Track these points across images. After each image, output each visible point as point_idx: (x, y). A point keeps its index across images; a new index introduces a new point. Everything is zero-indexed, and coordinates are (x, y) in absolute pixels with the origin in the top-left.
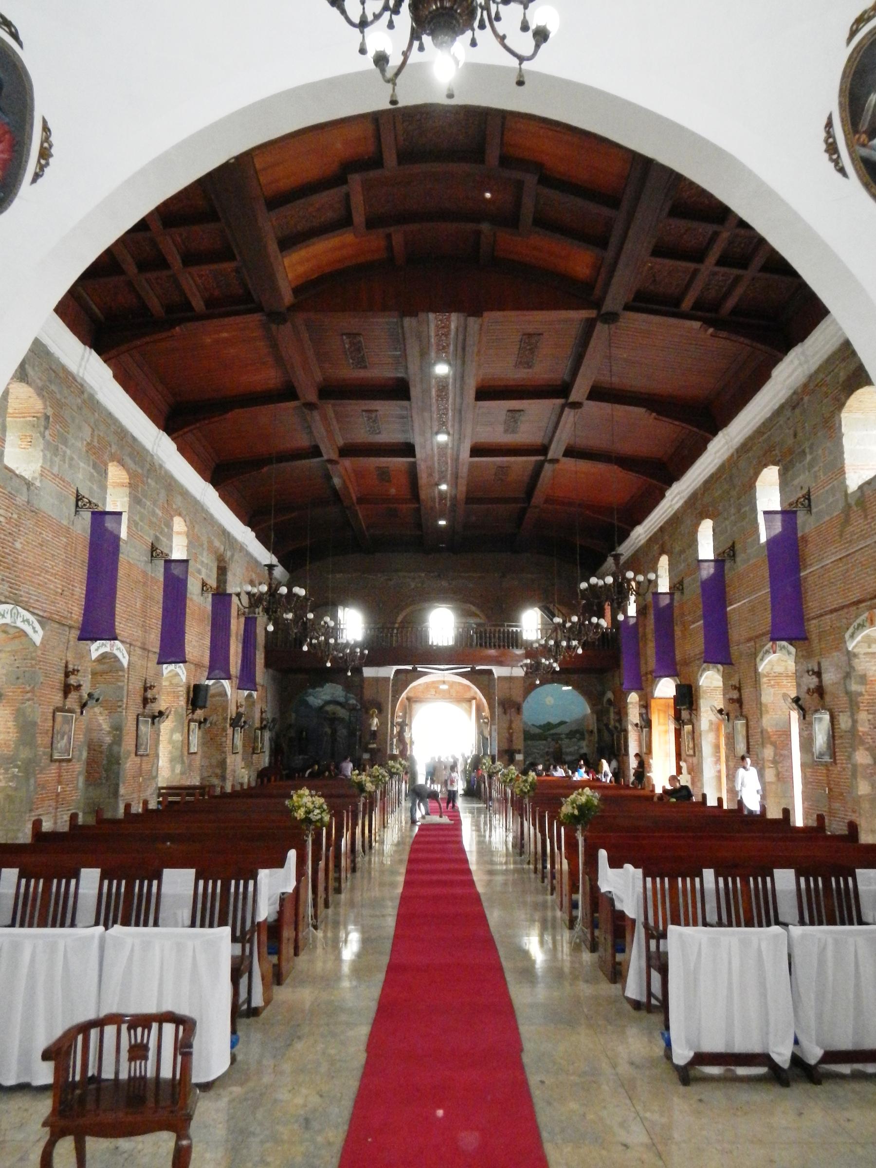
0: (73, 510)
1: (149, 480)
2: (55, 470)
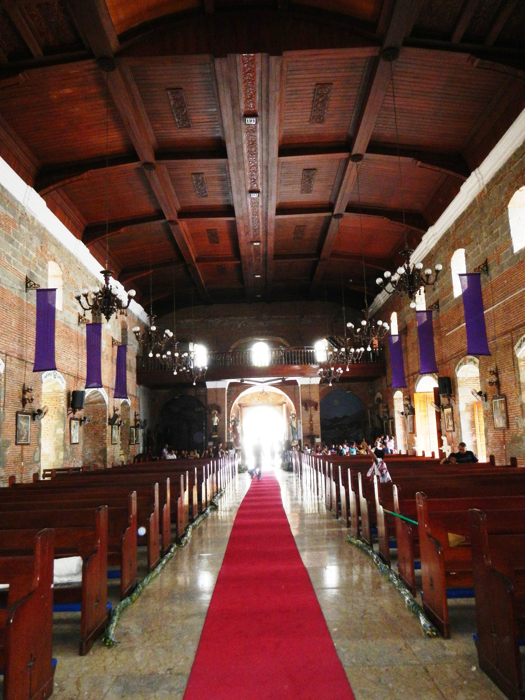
1: (21, 226)
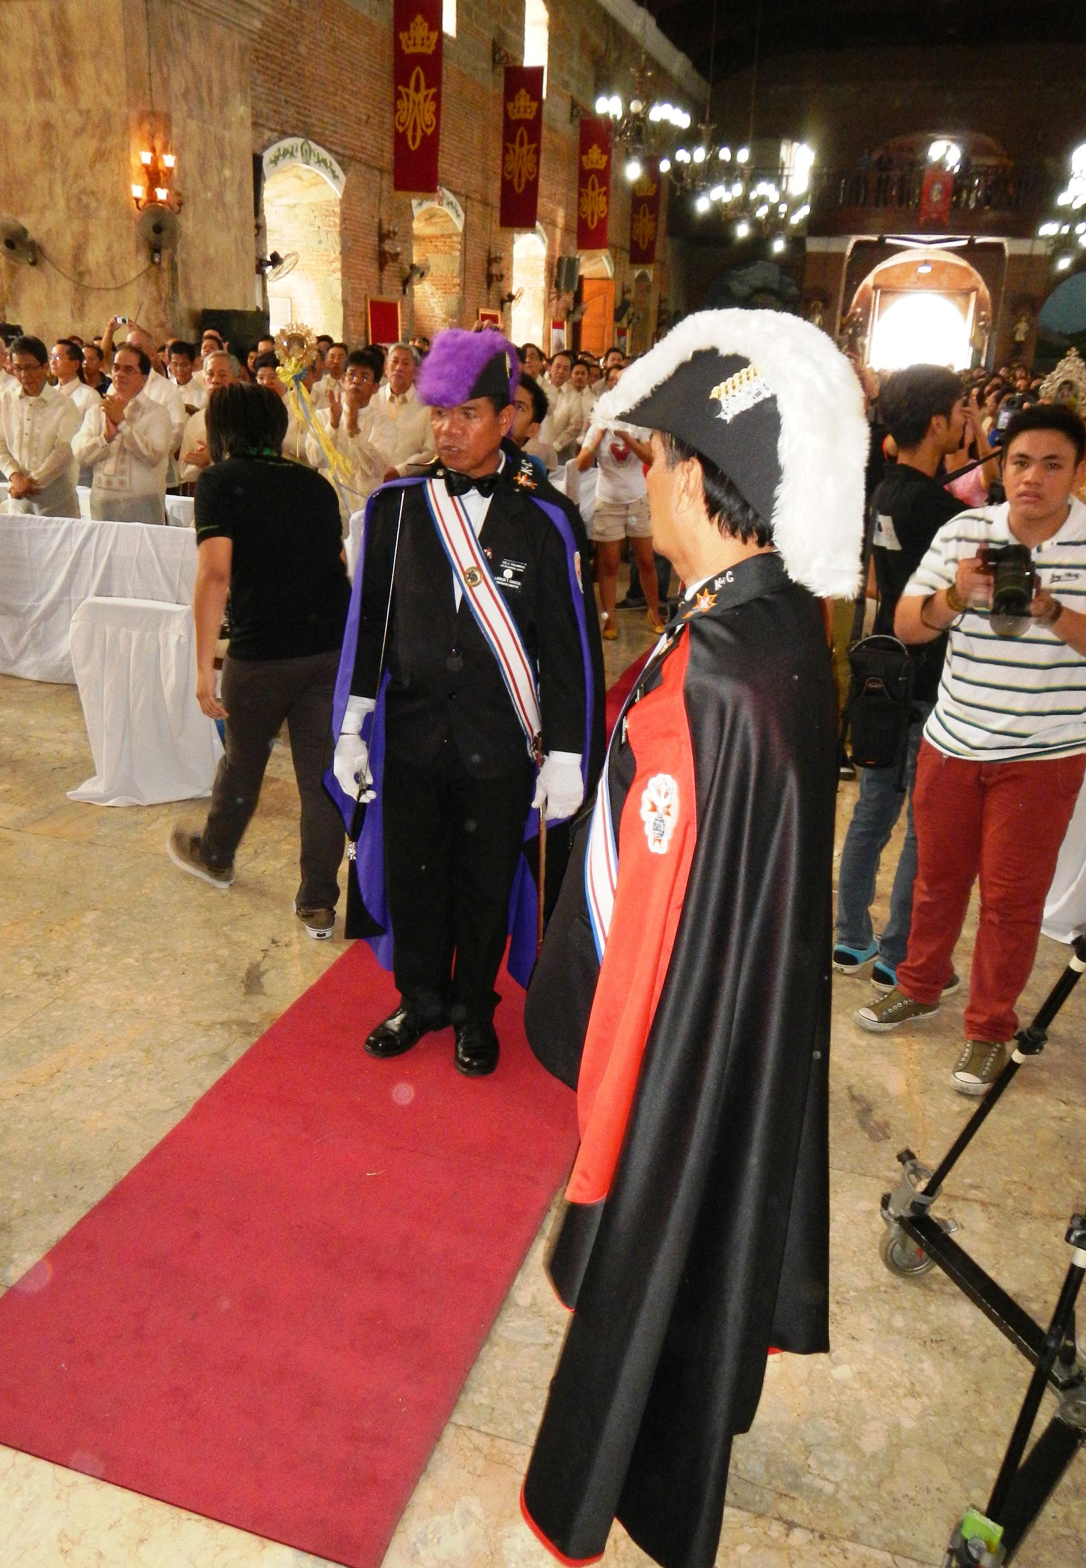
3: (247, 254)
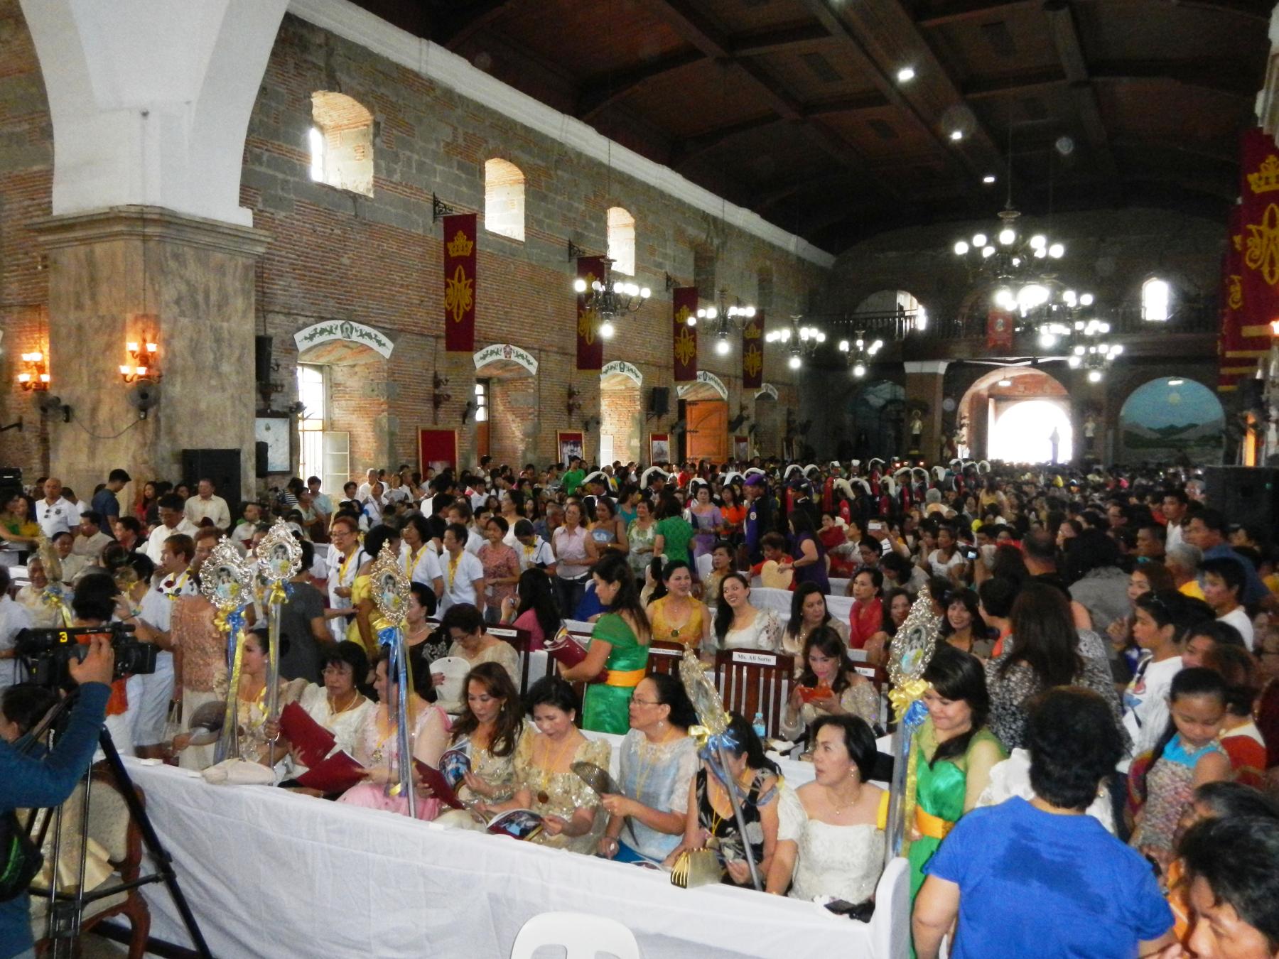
0: (431, 215)
1: (560, 173)
2: (397, 177)
3: (245, 405)
